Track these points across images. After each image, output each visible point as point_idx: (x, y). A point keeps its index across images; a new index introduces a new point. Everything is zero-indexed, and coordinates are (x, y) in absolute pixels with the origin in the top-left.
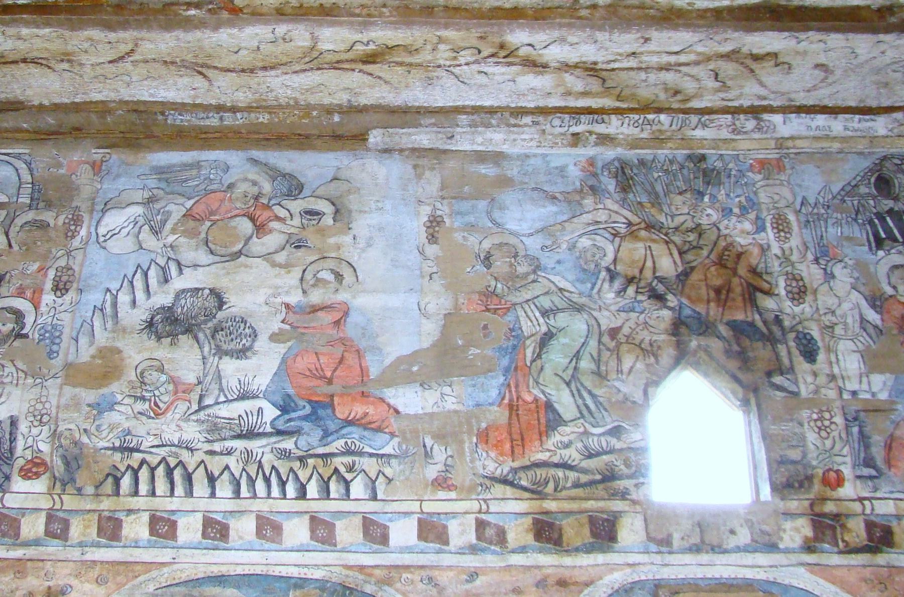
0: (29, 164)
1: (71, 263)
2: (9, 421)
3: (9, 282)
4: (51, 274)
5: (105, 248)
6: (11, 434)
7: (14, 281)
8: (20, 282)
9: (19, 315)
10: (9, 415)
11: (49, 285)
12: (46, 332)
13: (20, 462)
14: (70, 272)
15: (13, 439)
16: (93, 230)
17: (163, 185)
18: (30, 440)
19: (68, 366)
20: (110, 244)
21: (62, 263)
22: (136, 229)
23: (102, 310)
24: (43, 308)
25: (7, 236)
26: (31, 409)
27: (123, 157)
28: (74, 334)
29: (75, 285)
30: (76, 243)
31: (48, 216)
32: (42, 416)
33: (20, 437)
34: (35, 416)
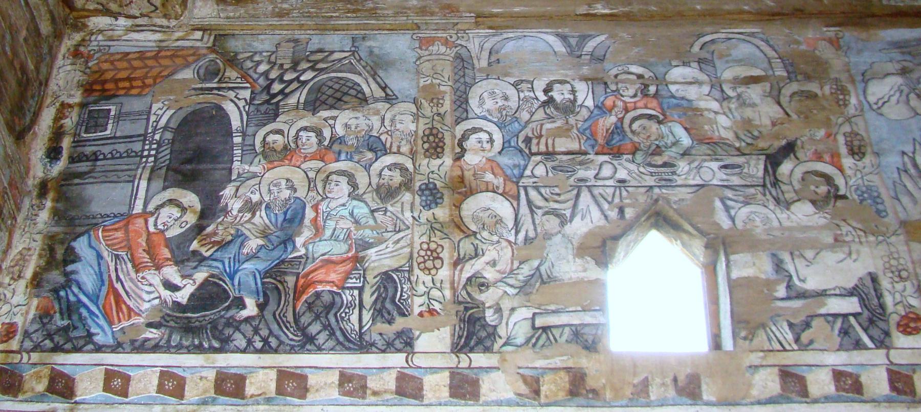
0: (767, 42)
1: (855, 128)
2: (869, 279)
3: (802, 148)
4: (841, 140)
5: (881, 115)
6: (875, 290)
7: (807, 146)
8: (814, 147)
9: (828, 179)
10: (866, 271)
11: (843, 150)
12: (863, 192)
13: (895, 318)
14: (858, 137)
15: (879, 296)
16: (862, 98)
17: (908, 58)
18: (898, 296)
19: (904, 224)
20: (885, 110)
21: (847, 128)
22: (904, 98)
23: (906, 171)
24: (849, 172)
25: (779, 103)
26: (887, 265)
27: (855, 34)
28: (892, 194)
29: (869, 149)
30: (851, 110)
31: (813, 87)
32: (900, 271)
33: (886, 294)
34: (892, 272)
